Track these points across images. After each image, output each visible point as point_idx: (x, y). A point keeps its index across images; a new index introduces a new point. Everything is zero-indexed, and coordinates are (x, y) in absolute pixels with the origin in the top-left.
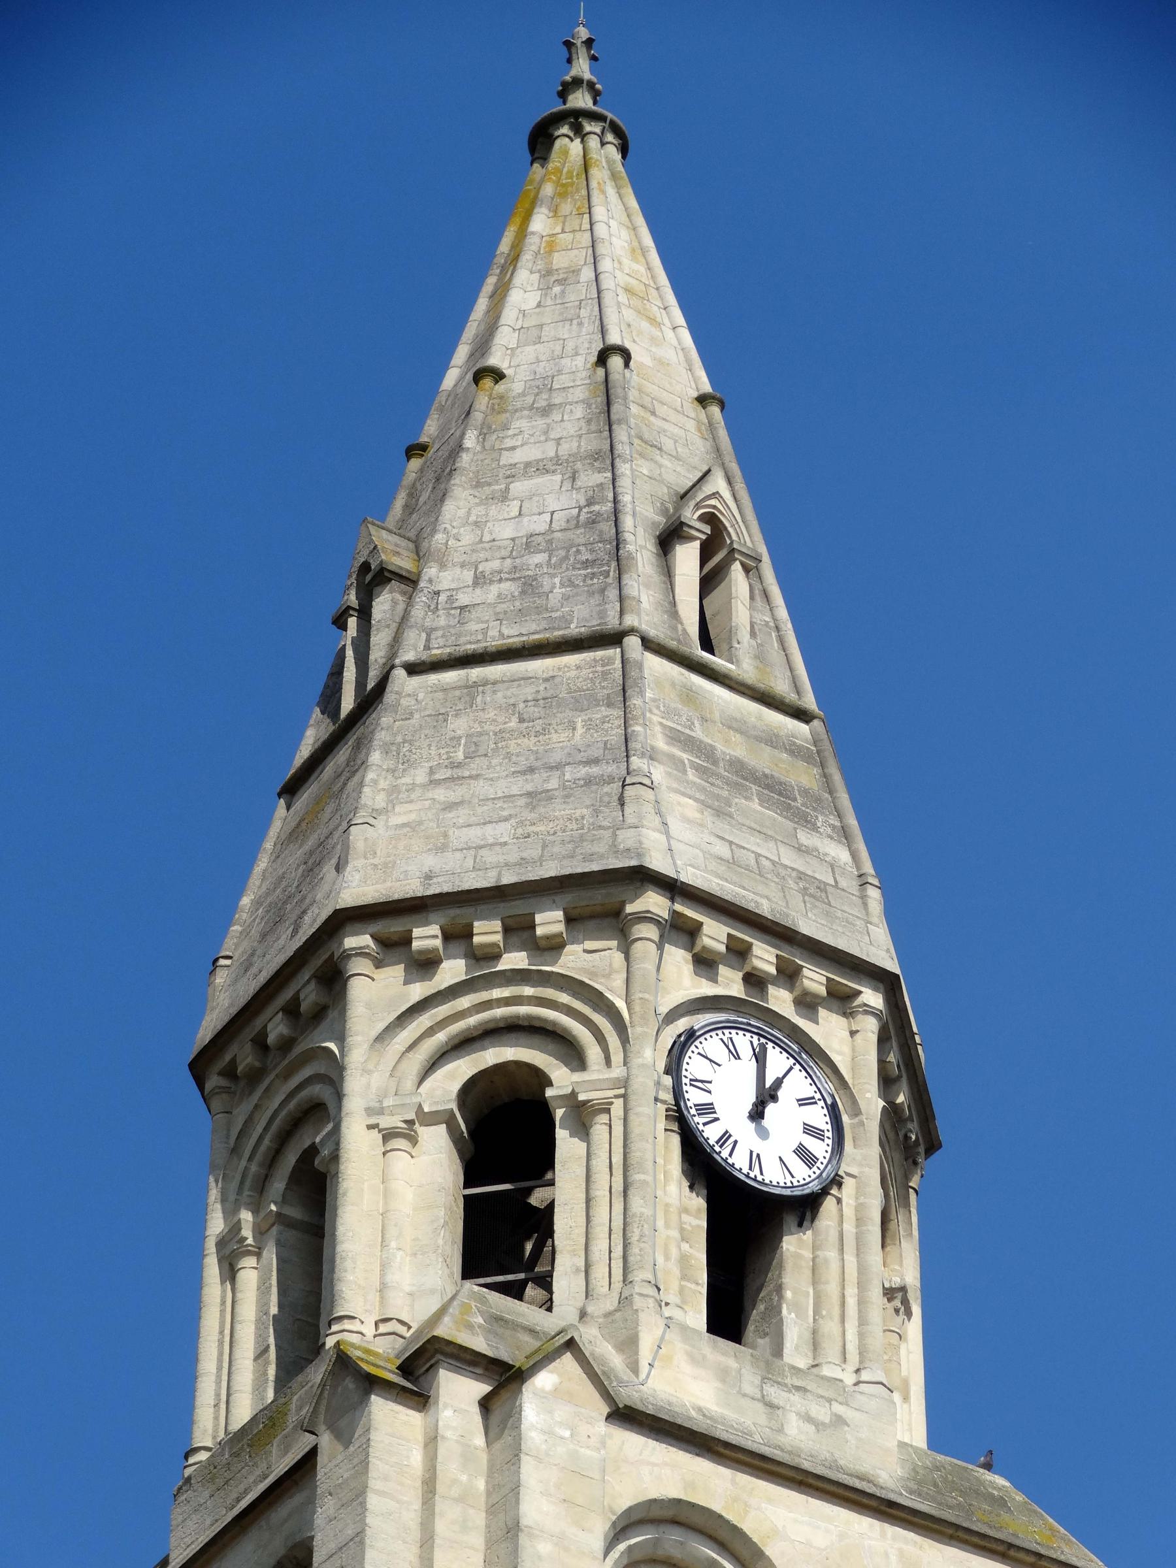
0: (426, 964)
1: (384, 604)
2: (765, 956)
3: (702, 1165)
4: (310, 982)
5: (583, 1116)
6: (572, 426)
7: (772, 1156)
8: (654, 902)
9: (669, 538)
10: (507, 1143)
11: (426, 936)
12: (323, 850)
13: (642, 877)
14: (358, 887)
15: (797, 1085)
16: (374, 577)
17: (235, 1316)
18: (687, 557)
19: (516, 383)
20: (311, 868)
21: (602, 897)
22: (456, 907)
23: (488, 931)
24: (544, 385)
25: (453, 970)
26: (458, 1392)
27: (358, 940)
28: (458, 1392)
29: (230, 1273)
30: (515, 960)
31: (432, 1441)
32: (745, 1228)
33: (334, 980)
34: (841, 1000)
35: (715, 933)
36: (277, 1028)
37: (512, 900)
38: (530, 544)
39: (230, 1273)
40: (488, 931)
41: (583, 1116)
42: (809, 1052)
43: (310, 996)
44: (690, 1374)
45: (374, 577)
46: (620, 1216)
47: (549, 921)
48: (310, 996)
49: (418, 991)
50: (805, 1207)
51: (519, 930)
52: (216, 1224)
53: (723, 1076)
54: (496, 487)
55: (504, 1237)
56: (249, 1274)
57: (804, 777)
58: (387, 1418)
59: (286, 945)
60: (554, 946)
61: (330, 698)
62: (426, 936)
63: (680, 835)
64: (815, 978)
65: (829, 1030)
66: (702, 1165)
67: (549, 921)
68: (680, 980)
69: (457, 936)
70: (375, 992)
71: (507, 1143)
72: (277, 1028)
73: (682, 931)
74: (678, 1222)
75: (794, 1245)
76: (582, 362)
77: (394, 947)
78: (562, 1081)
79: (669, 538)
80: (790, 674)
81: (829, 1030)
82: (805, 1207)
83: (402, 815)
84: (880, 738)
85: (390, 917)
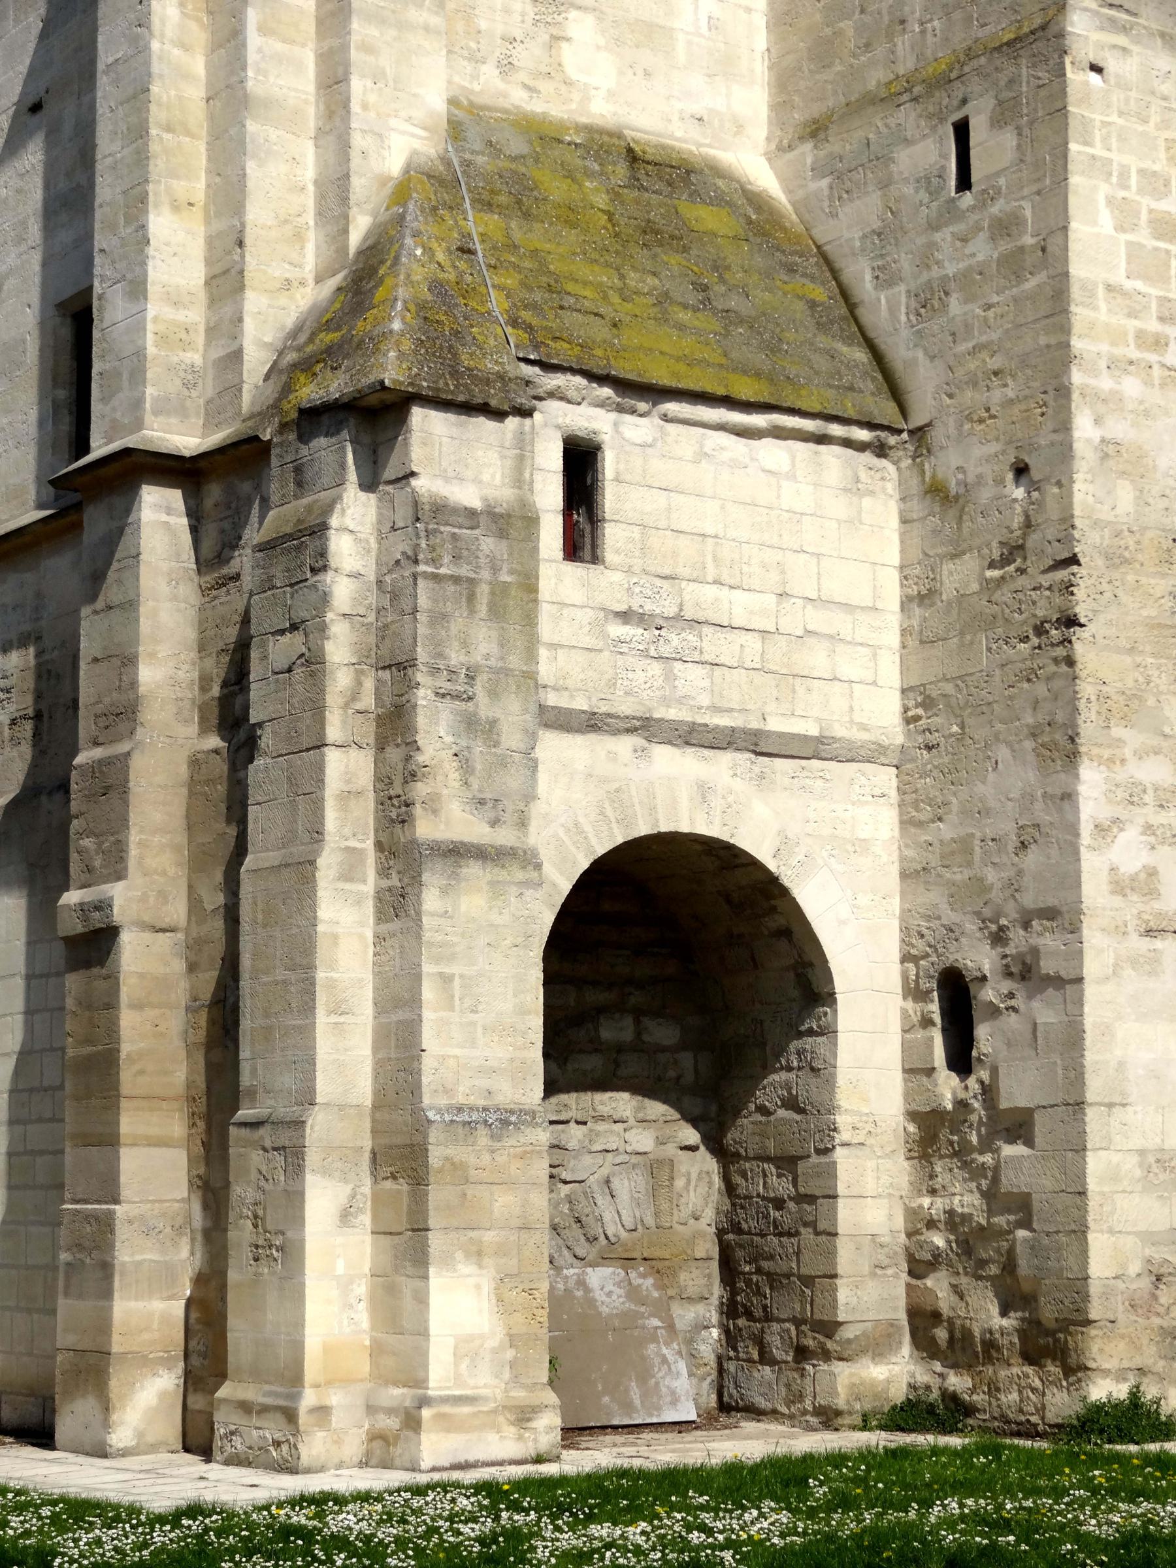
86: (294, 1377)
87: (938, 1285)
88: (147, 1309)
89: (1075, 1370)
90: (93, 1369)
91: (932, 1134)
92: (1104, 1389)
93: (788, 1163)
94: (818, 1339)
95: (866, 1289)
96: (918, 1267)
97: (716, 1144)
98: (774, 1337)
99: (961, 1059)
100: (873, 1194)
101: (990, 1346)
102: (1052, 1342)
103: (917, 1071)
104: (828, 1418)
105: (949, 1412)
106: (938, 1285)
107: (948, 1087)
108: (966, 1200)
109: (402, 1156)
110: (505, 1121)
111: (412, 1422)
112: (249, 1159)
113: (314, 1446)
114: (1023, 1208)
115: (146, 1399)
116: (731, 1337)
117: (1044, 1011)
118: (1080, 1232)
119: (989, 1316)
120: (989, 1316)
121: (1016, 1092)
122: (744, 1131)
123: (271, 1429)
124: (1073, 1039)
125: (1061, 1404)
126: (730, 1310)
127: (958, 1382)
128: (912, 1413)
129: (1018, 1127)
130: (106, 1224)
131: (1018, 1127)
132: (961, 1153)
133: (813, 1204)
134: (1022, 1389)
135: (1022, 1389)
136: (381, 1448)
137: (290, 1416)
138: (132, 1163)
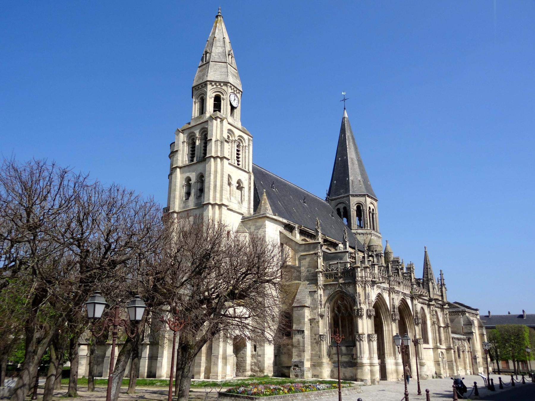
0: (213, 86)
1: (208, 55)
2: (235, 89)
3: (231, 104)
4: (204, 84)
5: (223, 99)
6: (222, 43)
7: (235, 104)
8: (229, 85)
9: (229, 55)
10: (218, 100)
11: (213, 83)
12: (206, 74)
13: (229, 83)
14: (209, 79)
15: (236, 99)
16: (206, 53)
17: (196, 108)
18: (230, 56)
19: (217, 38)
20: (203, 75)
21: (226, 83)
22: (216, 82)
23: (218, 84)
24: (219, 39)
25: (215, 86)
26: (219, 120)
27: (208, 83)
28: (219, 120)
29: (195, 104)
30: (219, 87)
31: (217, 123)
32: (233, 108)
33: (206, 85)
34: (239, 93)
35: (233, 87)
36: (200, 87)
37: (220, 82)
38: (219, 53)
39: (195, 104)
40: (218, 84)
41: (223, 99)
42: (237, 96)
43: (204, 86)
44: (230, 120)
45: (206, 53)
46: (225, 106)
47: (222, 84)
48: (204, 86)
49: (212, 87)
50: (236, 108)
51: (220, 85)
52: (194, 100)
53: (232, 97)
54: (216, 47)
55: (217, 106)
56: (197, 104)
57: (237, 75)
58: (214, 121)
59: (201, 81)
60: (222, 86)
61: (202, 60)
62: (213, 83)
63: (231, 80)
64: (238, 91)
65: (238, 95)
66: (231, 104)
67: (222, 84)
68: (230, 90)
69: (215, 84)
70: (209, 87)
71: (218, 100)
72: (200, 87)
73: (231, 87)
74: (229, 107)
75: (235, 110)
76: (222, 38)
77: (211, 84)
78: (222, 96)
79: (229, 55)
80: (235, 66)
81: (238, 95)
82: (236, 108)
83: (212, 73)
84: (242, 74)
85: (211, 82)
86: (217, 373)
87: (253, 367)
88: (203, 369)
89: (263, 373)
90: (199, 373)
91: (253, 356)
92: (265, 374)
93: (242, 358)
94: (245, 371)
95: (248, 367)
96: (251, 365)
97: (236, 356)
98: (241, 371)
99: (255, 351)
100: (249, 360)
101: (257, 371)
102: (262, 371)
103: (252, 351)
104: (245, 376)
105: (254, 376)
106: (253, 367)
107: (254, 353)
108: (255, 361)
109: (225, 358)
110: (231, 356)
111: (225, 376)
112: (213, 359)
113: (219, 378)
114: (260, 362)
115: (202, 375)
116: (237, 371)
117: (262, 348)
118: (264, 363)
119: (257, 369)
120: (257, 369)
121: (260, 353)
122: (239, 355)
123: (215, 377)
124: (264, 350)
125: (262, 375)
126: (237, 369)
127: (254, 374)
128: (251, 376)
129: (260, 356)
130: (200, 362)
131: (260, 356)
132: (255, 357)
133: (245, 361)
134: (259, 374)
135: (259, 374)
136: (223, 378)
137: (217, 376)
138: (202, 358)
